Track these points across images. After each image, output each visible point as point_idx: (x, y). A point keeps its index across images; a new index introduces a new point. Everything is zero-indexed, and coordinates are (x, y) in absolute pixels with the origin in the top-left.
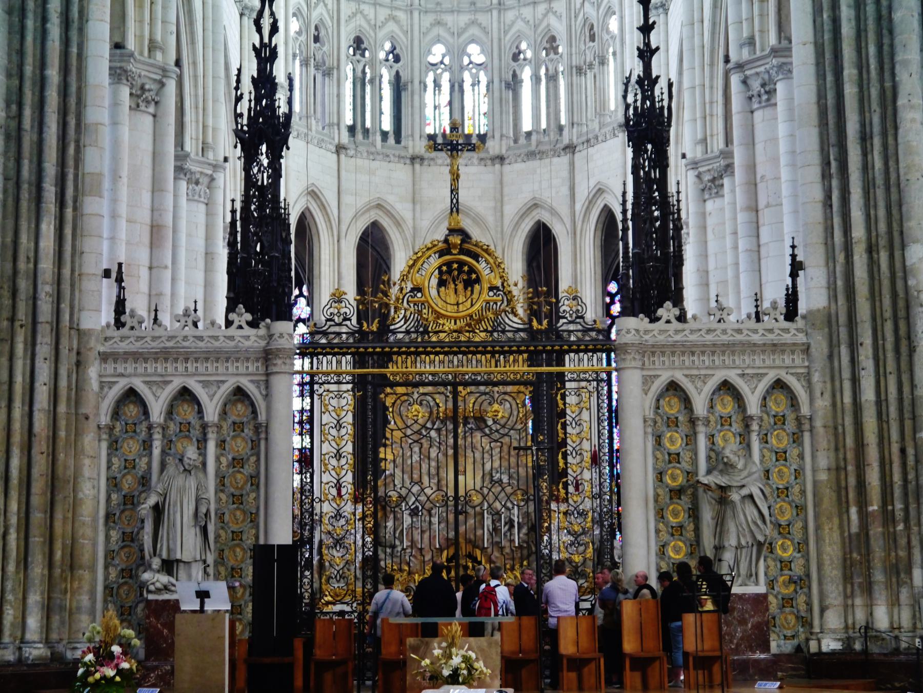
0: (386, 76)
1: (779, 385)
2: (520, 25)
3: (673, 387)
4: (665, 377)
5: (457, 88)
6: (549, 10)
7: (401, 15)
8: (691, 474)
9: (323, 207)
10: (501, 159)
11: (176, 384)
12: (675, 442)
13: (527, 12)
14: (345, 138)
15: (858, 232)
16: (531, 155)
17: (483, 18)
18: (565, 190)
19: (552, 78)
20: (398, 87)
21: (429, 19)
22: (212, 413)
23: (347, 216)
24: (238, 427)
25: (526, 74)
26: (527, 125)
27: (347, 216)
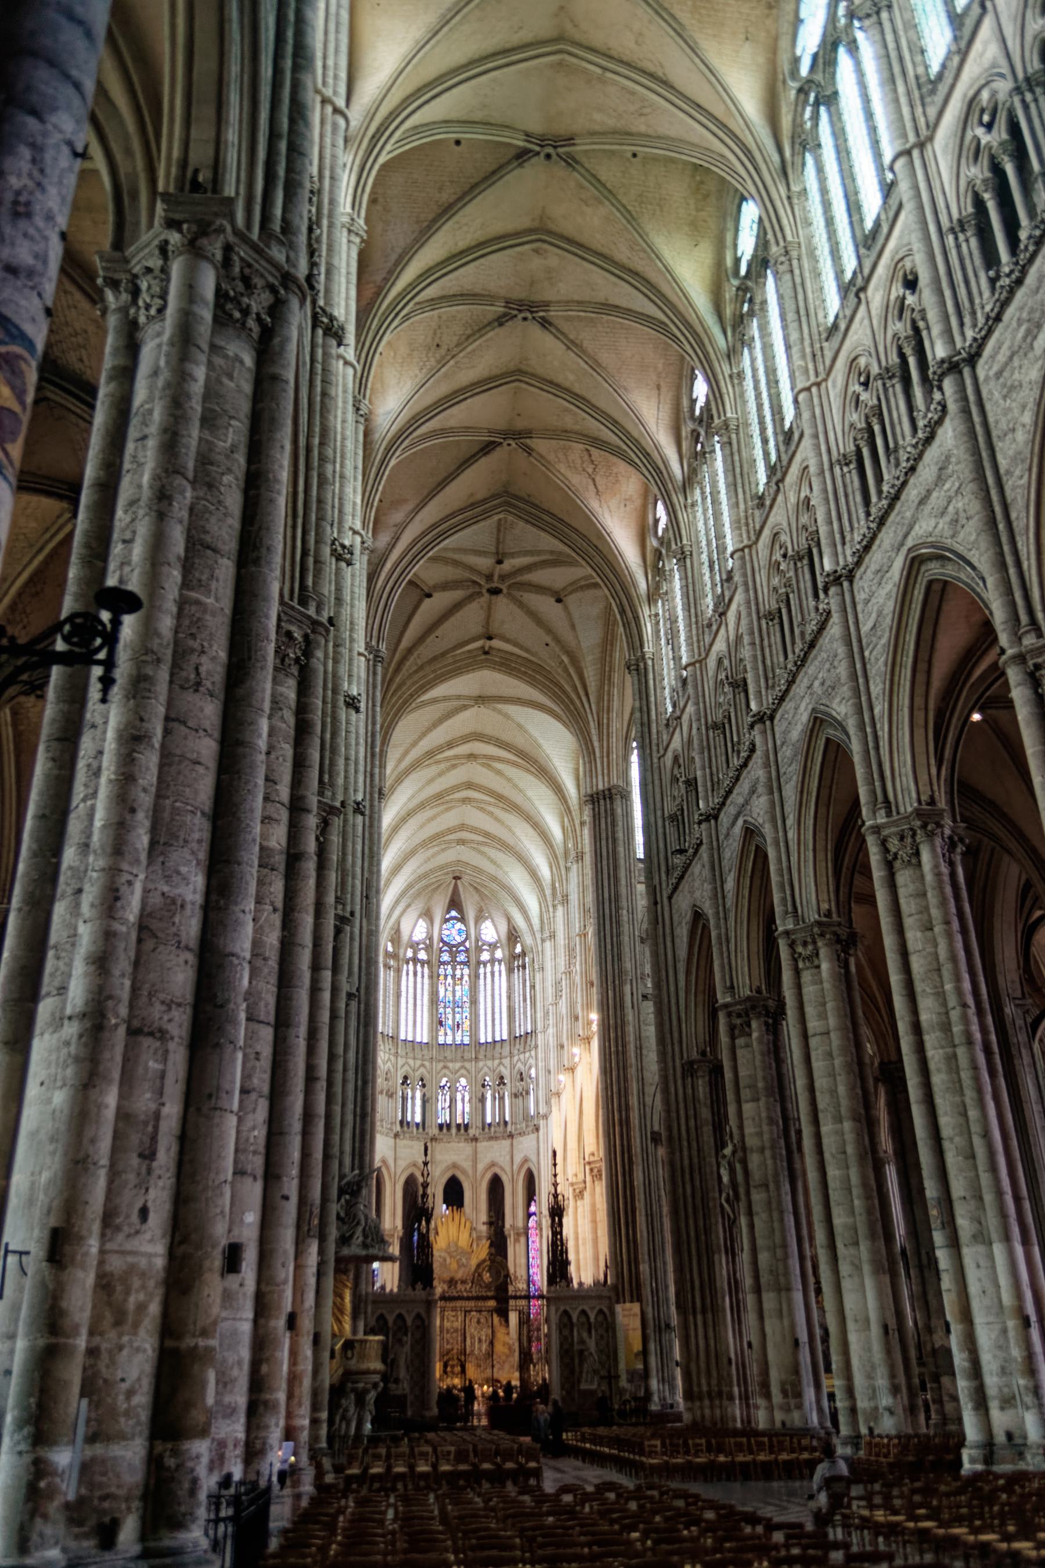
0: (418, 1095)
1: (601, 1311)
2: (486, 1069)
3: (565, 1312)
4: (562, 1308)
5: (453, 1101)
6: (501, 1063)
7: (427, 1064)
8: (572, 1344)
9: (388, 1168)
10: (475, 1139)
11: (397, 1312)
12: (566, 1332)
13: (489, 1063)
14: (398, 1128)
15: (625, 1257)
16: (491, 1138)
17: (467, 1065)
18: (508, 1158)
19: (502, 1099)
20: (424, 1102)
21: (441, 1064)
22: (409, 1321)
23: (399, 1171)
24: (418, 1327)
25: (489, 1095)
26: (489, 1120)
27: (399, 1171)
